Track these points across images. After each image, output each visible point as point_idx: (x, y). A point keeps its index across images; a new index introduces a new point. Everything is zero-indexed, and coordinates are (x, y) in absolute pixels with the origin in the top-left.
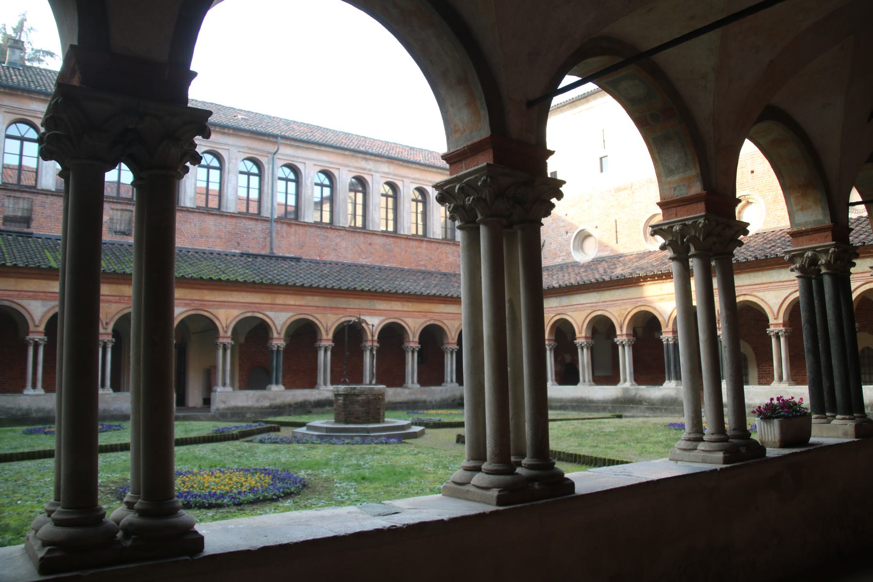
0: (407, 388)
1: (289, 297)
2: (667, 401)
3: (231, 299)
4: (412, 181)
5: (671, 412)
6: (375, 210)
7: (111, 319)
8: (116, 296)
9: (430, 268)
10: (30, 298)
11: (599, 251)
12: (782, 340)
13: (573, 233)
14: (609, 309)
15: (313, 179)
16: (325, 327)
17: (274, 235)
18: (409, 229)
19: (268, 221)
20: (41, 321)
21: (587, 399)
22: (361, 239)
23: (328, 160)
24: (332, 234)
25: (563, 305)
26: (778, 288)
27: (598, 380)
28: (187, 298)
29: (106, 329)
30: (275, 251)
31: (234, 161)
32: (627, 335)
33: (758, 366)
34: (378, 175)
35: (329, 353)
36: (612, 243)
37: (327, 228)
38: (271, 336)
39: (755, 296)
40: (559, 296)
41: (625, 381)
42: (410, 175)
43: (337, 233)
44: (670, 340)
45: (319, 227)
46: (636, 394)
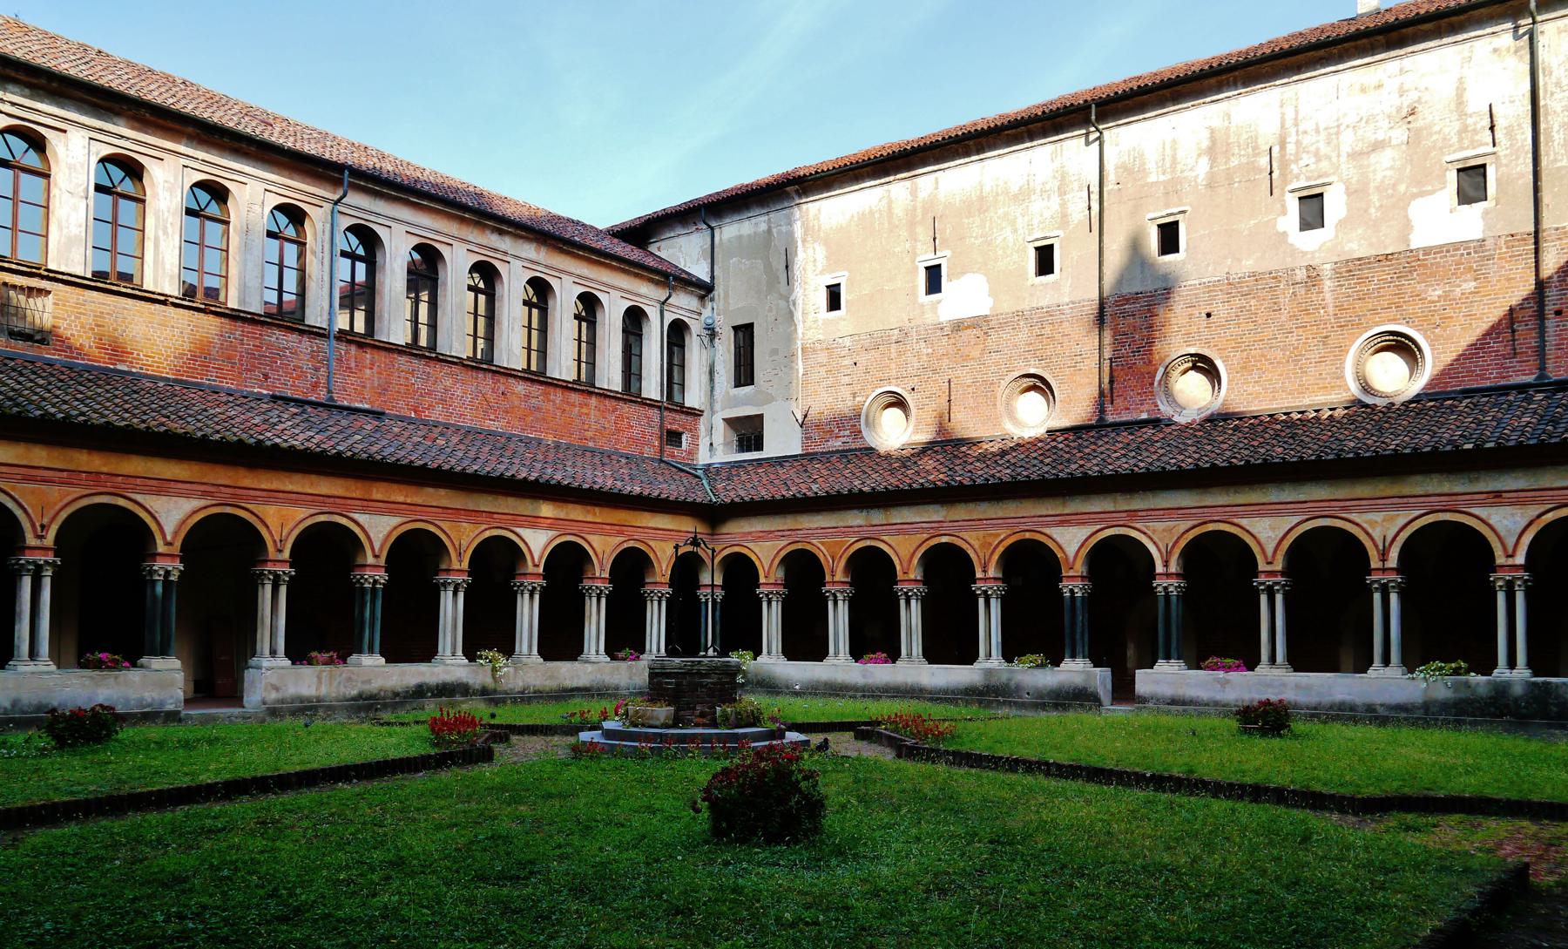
0: (587, 662)
1: (395, 486)
3: (290, 487)
4: (576, 280)
6: (513, 329)
7: (53, 519)
12: (1279, 598)
16: (457, 546)
19: (323, 336)
22: (486, 383)
23: (432, 226)
25: (874, 523)
26: (1277, 514)
27: (935, 653)
28: (205, 480)
29: (41, 537)
42: (572, 270)
43: (447, 369)
45: (415, 355)
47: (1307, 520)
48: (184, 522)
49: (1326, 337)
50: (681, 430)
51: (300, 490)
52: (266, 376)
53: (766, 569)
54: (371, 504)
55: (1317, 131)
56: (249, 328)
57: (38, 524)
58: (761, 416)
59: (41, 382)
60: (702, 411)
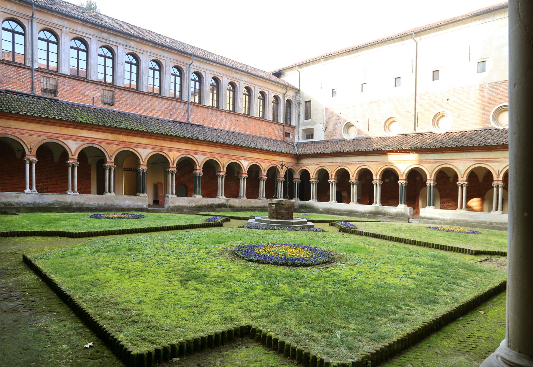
1: (205, 147)
2: (399, 214)
3: (176, 147)
4: (259, 87)
5: (401, 220)
8: (116, 141)
9: (266, 136)
10: (69, 139)
13: (344, 123)
14: (370, 166)
15: (209, 81)
16: (222, 164)
17: (189, 111)
18: (257, 113)
19: (186, 103)
20: (75, 153)
21: (355, 211)
22: (233, 117)
24: (219, 114)
26: (465, 162)
27: (360, 201)
28: (153, 144)
29: (111, 159)
30: (190, 121)
31: (168, 67)
32: (379, 180)
33: (441, 200)
34: (242, 82)
35: (224, 179)
36: (366, 131)
37: (216, 110)
38: (195, 168)
40: (342, 157)
41: (376, 203)
42: (258, 84)
43: (221, 113)
44: (403, 184)
45: (212, 109)
48: (147, 156)
50: (289, 132)
51: (179, 148)
52: (171, 115)
54: (198, 152)
56: (166, 101)
57: (110, 156)
59: (111, 116)
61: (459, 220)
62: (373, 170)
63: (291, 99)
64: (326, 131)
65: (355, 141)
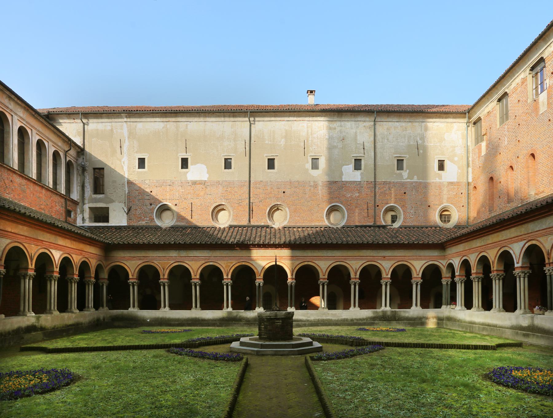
0: (72, 312)
11: (177, 221)
13: (157, 205)
25: (182, 256)
26: (326, 260)
36: (189, 217)
39: (314, 263)
41: (227, 307)
46: (237, 316)
47: (335, 262)
49: (319, 204)
50: (71, 210)
53: (133, 272)
55: (318, 138)
58: (107, 209)
60: (79, 203)
61: (323, 319)
62: (223, 268)
63: (72, 161)
64: (130, 213)
65: (174, 228)
